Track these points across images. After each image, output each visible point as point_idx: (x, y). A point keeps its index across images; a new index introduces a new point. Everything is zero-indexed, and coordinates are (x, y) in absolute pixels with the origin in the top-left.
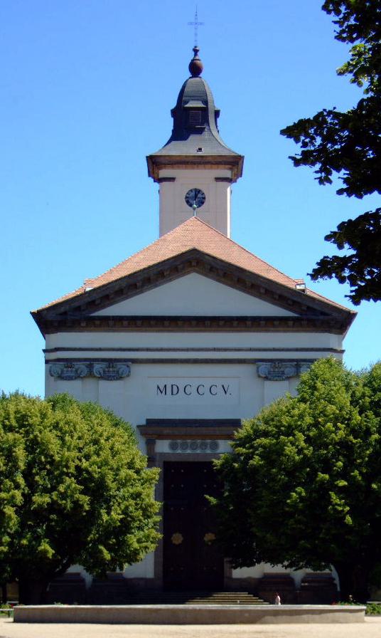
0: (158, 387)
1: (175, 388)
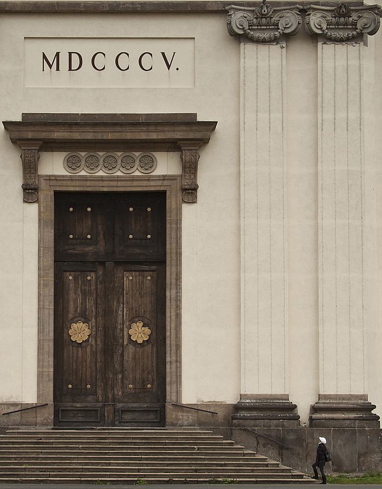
0: (44, 57)
1: (75, 58)
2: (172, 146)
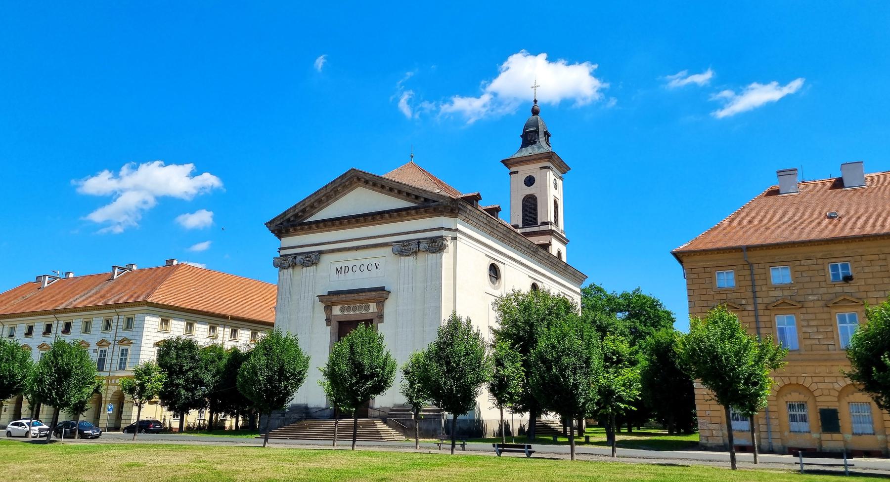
0: (337, 269)
1: (347, 268)
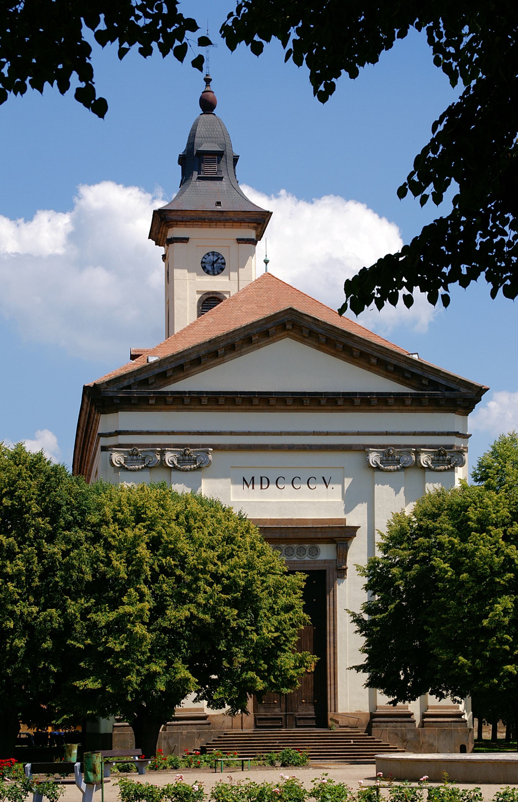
0: (244, 480)
1: (265, 480)
2: (330, 540)
